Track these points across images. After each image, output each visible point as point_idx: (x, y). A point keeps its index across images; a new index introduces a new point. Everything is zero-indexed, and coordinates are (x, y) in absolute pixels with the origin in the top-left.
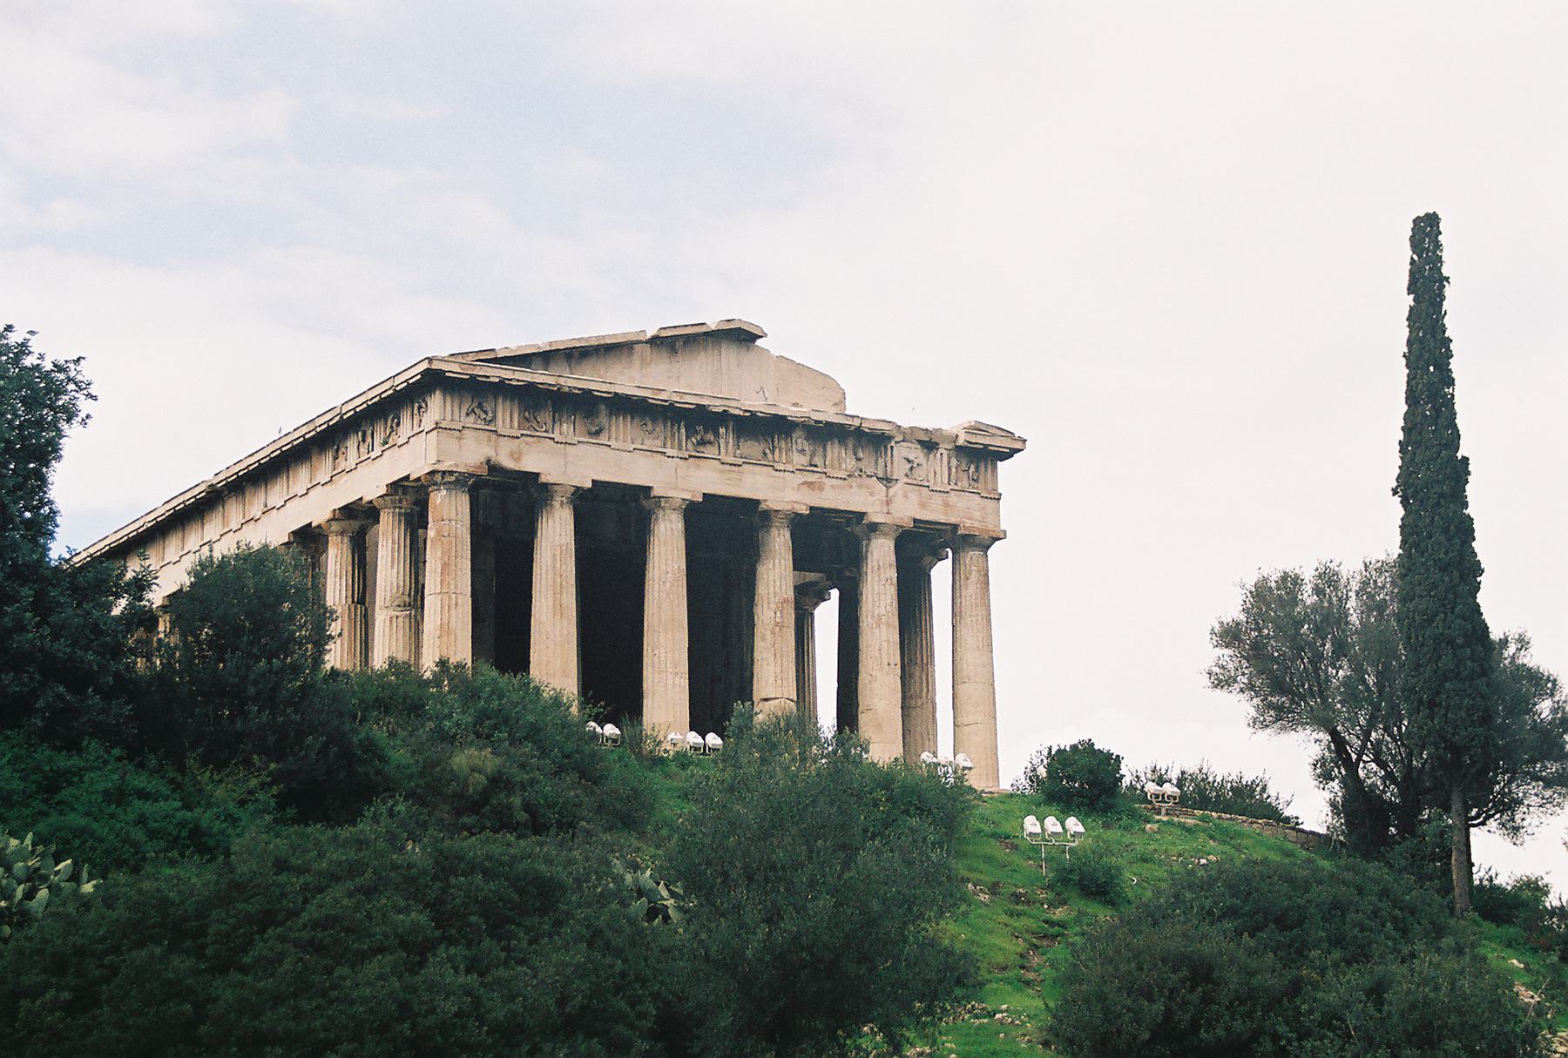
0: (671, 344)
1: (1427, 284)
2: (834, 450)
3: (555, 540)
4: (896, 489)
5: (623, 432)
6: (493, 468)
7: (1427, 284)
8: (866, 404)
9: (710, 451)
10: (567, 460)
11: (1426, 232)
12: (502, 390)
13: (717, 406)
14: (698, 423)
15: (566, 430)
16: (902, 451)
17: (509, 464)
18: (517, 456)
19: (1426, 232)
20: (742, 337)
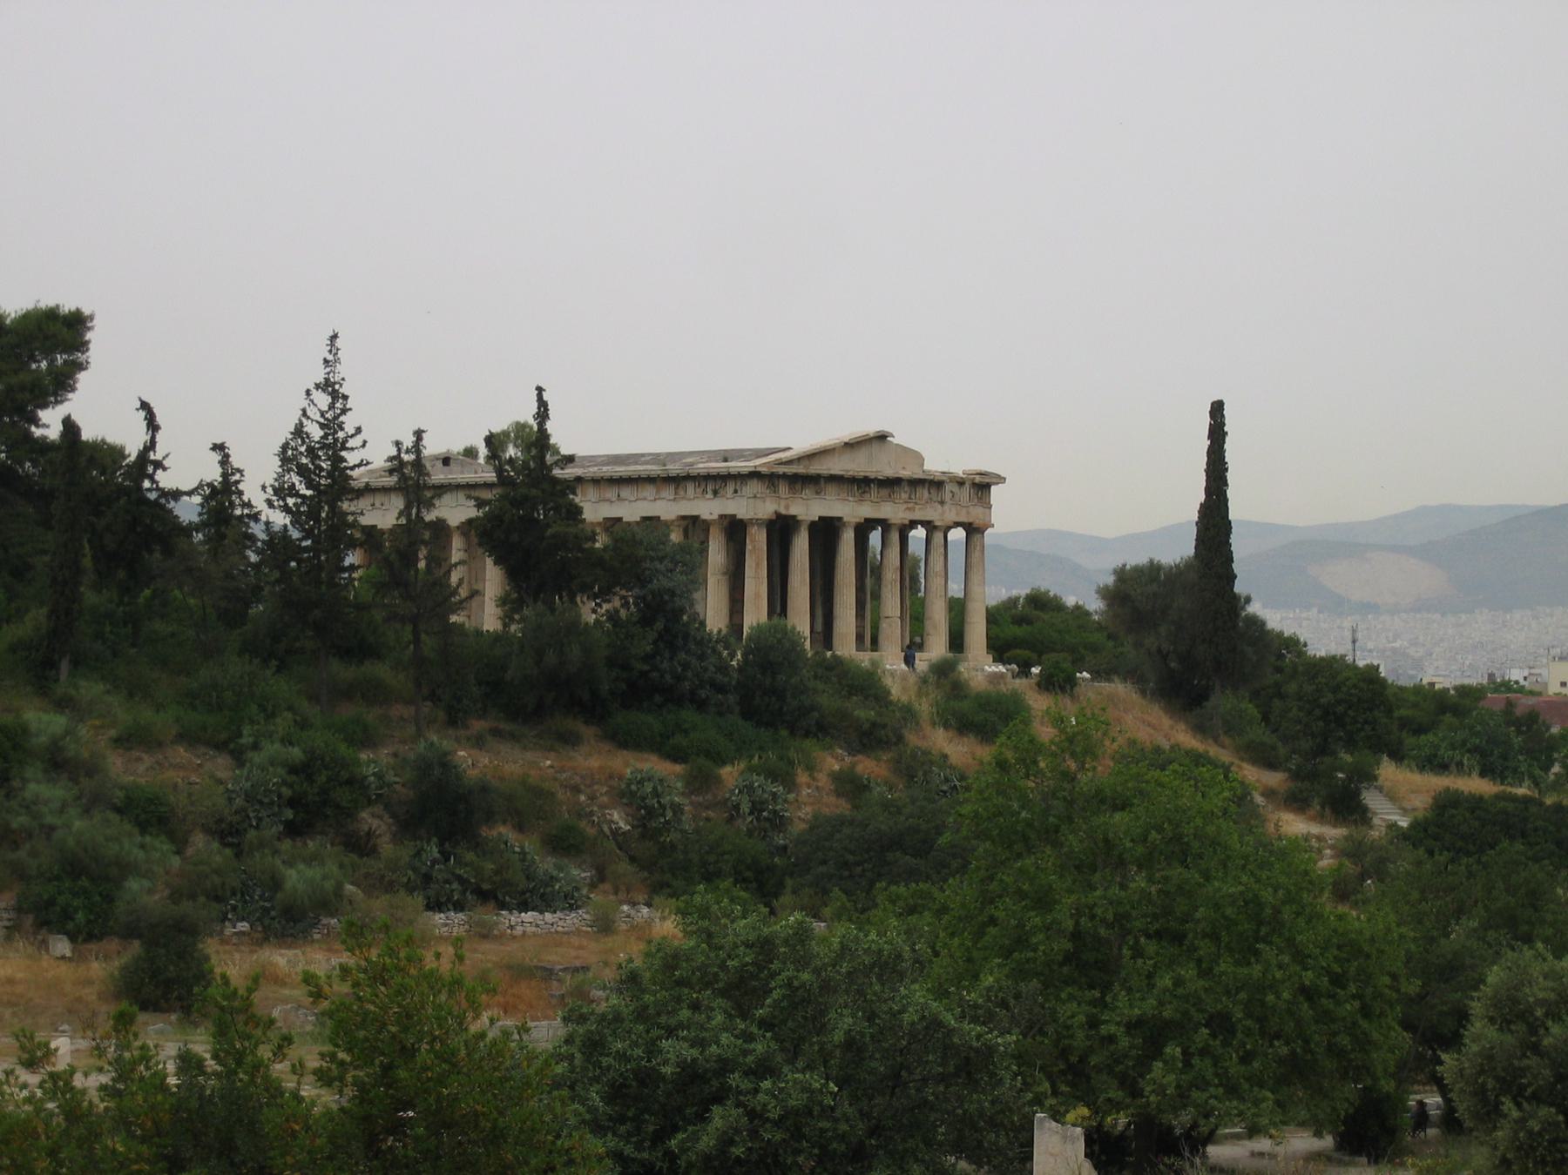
0: (851, 446)
1: (1217, 434)
2: (919, 490)
3: (801, 545)
4: (946, 507)
5: (831, 491)
6: (778, 515)
7: (1217, 434)
8: (935, 464)
9: (867, 496)
10: (808, 508)
11: (1217, 409)
12: (784, 476)
13: (872, 476)
14: (861, 484)
15: (808, 492)
16: (948, 487)
17: (783, 512)
18: (787, 507)
19: (1217, 409)
20: (882, 437)
